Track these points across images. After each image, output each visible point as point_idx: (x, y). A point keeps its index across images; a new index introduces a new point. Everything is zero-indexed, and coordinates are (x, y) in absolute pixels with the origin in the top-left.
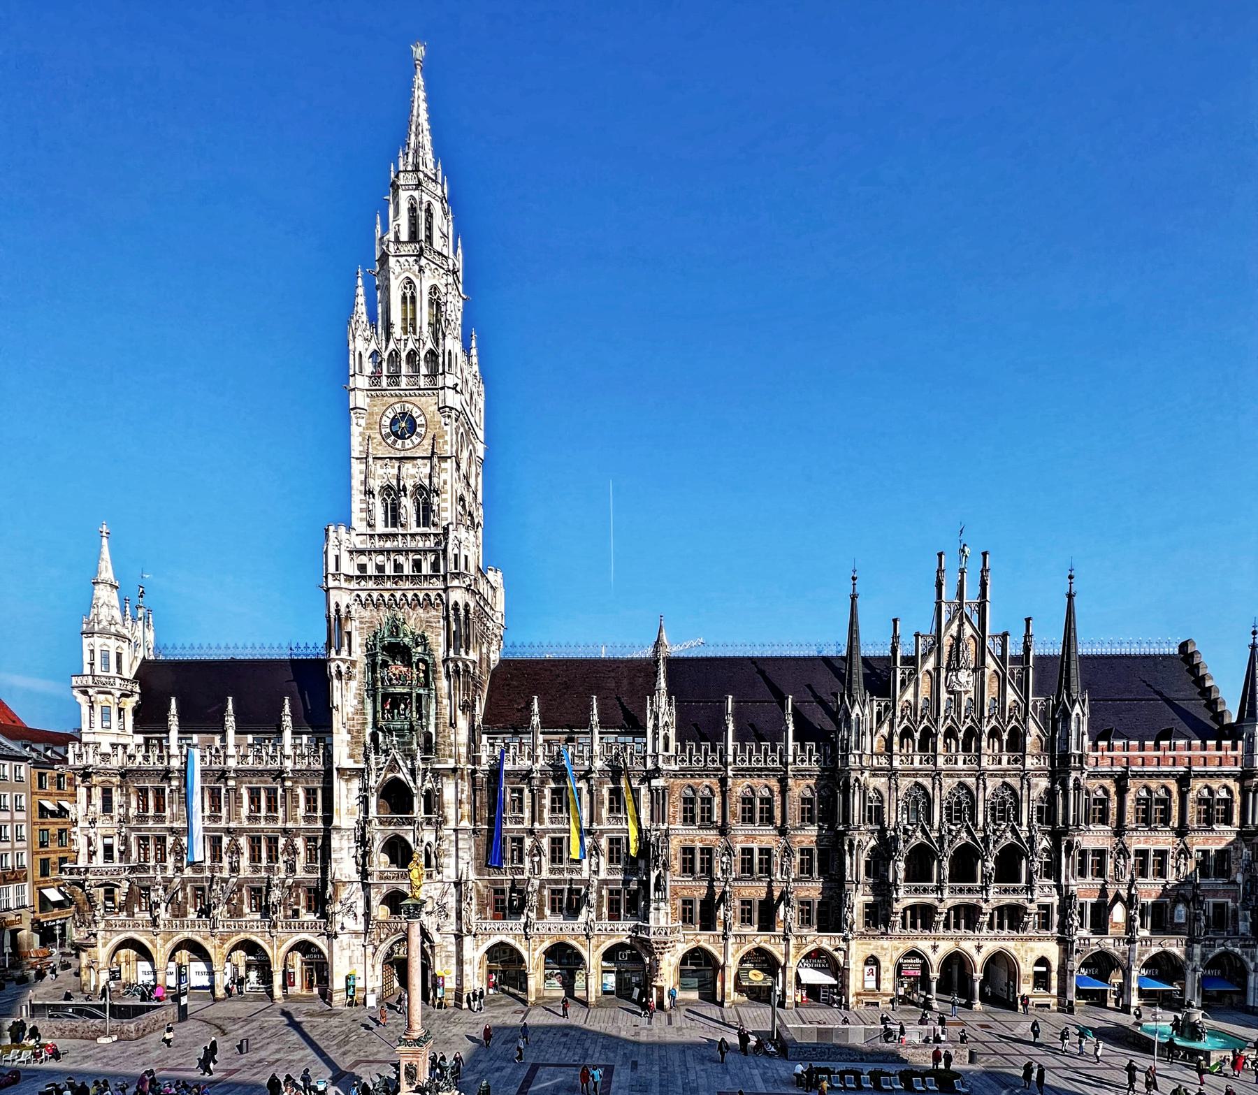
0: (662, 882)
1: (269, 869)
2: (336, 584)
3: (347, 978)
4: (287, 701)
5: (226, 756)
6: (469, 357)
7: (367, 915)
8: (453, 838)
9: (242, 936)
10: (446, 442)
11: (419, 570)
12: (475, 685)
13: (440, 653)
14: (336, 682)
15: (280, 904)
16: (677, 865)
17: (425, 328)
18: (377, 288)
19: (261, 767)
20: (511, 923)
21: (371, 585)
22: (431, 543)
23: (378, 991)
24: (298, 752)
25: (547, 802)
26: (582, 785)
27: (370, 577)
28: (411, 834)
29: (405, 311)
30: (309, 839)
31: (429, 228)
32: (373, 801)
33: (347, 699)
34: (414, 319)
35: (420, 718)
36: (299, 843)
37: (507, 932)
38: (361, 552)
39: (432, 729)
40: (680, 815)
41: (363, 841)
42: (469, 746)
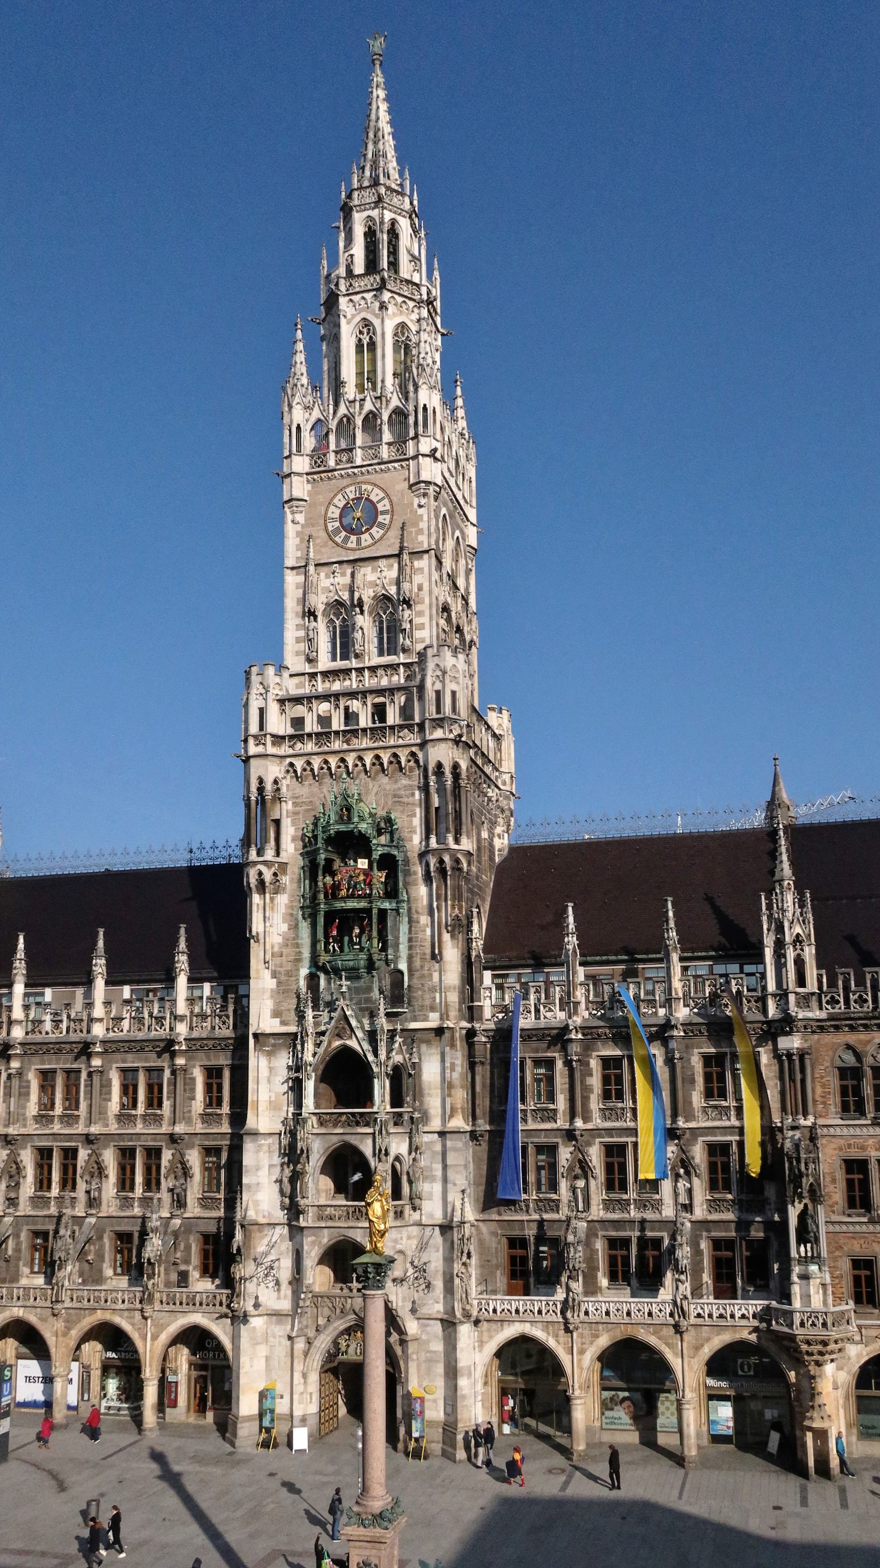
0: (811, 1226)
1: (146, 1202)
2: (260, 749)
3: (262, 1395)
4: (182, 931)
5: (91, 1020)
6: (453, 410)
7: (297, 1279)
8: (438, 1147)
9: (100, 1316)
10: (421, 532)
11: (383, 719)
12: (470, 890)
13: (416, 841)
14: (256, 898)
15: (160, 1262)
16: (836, 1192)
17: (390, 380)
18: (323, 338)
19: (140, 1035)
20: (537, 1301)
21: (310, 747)
22: (399, 679)
23: (313, 1421)
24: (197, 1010)
25: (595, 1082)
26: (657, 1051)
27: (310, 735)
28: (370, 1141)
29: (360, 363)
30: (208, 1151)
31: (394, 252)
32: (309, 1086)
33: (274, 923)
34: (373, 371)
35: (384, 949)
36: (194, 1158)
37: (532, 1317)
38: (297, 700)
39: (403, 966)
40: (834, 1101)
41: (293, 1155)
42: (462, 992)
